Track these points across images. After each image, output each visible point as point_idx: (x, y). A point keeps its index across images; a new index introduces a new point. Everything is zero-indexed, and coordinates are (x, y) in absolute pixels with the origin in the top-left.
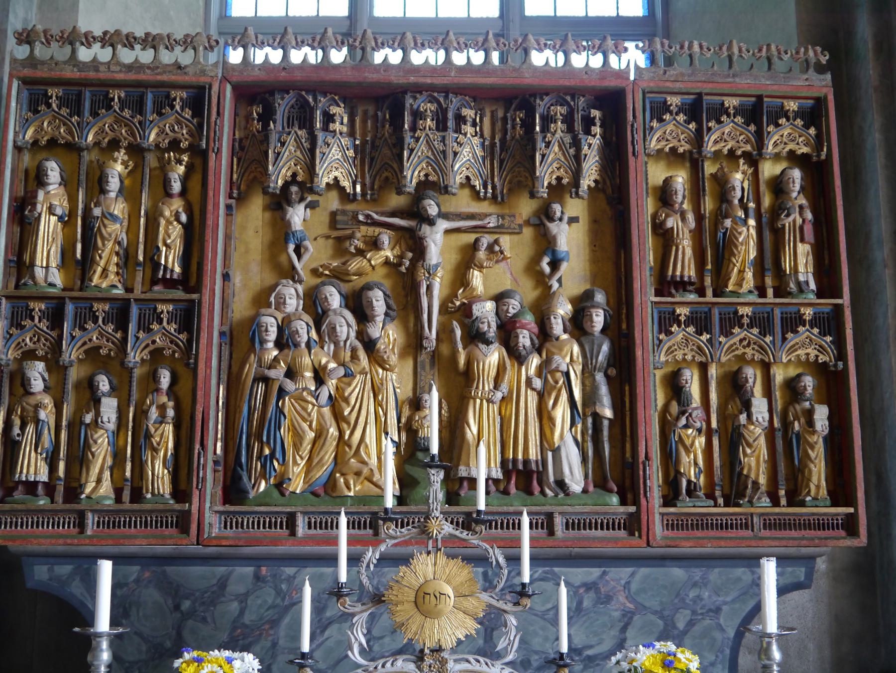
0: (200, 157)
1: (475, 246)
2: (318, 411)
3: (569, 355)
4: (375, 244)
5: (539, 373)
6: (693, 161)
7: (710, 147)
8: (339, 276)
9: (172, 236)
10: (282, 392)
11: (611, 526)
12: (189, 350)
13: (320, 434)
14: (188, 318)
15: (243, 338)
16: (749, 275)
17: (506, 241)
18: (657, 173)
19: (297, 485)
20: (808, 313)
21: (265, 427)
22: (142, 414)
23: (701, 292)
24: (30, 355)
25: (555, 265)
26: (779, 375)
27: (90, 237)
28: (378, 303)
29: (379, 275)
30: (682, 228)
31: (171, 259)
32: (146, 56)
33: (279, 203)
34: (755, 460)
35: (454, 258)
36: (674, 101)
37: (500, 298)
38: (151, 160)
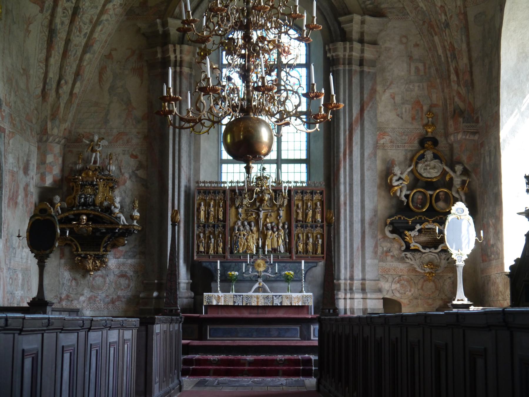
0: (225, 202)
1: (267, 215)
2: (244, 240)
3: (282, 233)
4: (252, 215)
5: (277, 234)
6: (302, 200)
7: (305, 198)
8: (247, 219)
9: (221, 213)
10: (238, 238)
11: (287, 257)
12: (224, 231)
13: (244, 244)
14: (224, 227)
15: (232, 229)
16: (310, 219)
17: (272, 214)
18: (296, 202)
19: (241, 252)
20: (319, 225)
21: (236, 243)
22: (217, 241)
23: (303, 222)
24: (201, 232)
25: (280, 218)
26: (315, 235)
27: (209, 213)
28: (253, 224)
29: (253, 220)
30: (300, 212)
31: (221, 217)
32: (216, 185)
33: (237, 208)
34: (310, 248)
35: (264, 216)
36: (299, 191)
37: (271, 223)
38: (217, 201)
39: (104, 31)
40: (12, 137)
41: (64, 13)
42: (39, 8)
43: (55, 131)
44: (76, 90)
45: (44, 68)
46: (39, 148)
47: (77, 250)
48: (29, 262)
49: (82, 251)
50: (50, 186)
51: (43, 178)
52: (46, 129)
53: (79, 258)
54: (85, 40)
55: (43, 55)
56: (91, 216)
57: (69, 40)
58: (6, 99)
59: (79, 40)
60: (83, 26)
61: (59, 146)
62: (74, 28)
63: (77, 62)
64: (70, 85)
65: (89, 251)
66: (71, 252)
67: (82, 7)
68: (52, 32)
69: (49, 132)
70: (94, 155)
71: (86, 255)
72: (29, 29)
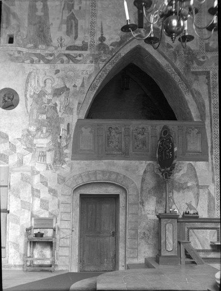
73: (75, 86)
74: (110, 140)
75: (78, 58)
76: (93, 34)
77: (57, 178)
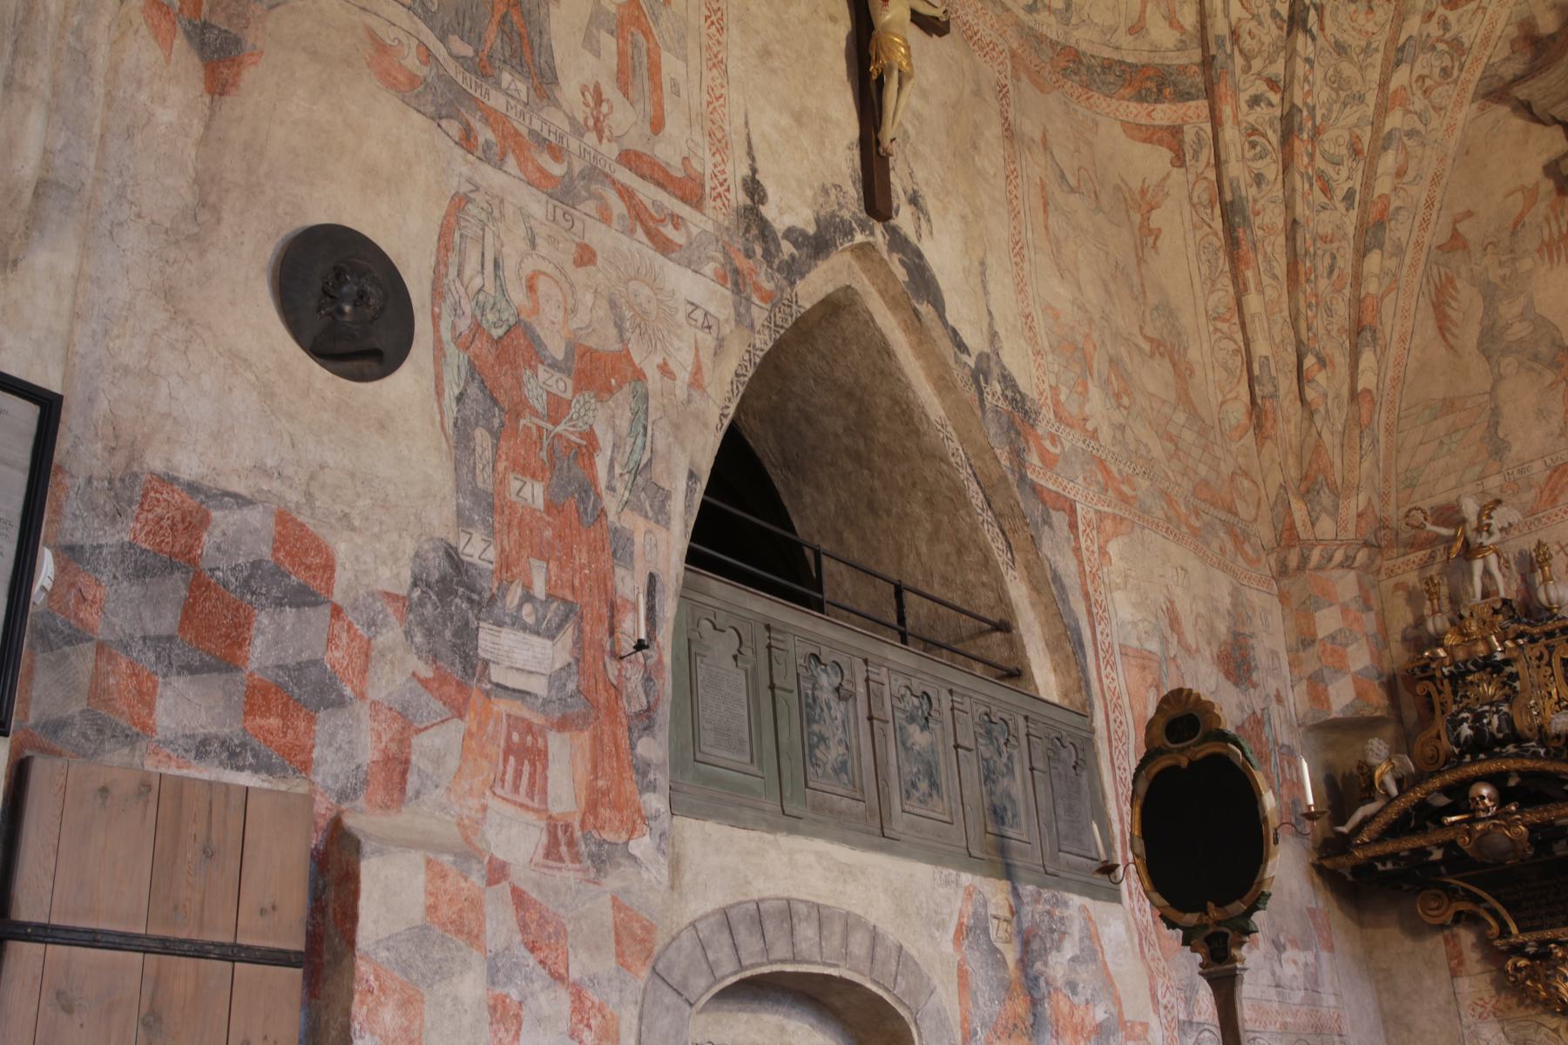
39: (1411, 174)
40: (1116, 534)
41: (1253, 145)
42: (1167, 154)
43: (1326, 527)
44: (1366, 381)
45: (1239, 337)
46: (1283, 598)
47: (1504, 932)
48: (1329, 1000)
49: (1521, 931)
50: (1349, 714)
51: (1317, 692)
52: (1292, 527)
53: (1522, 963)
54: (1354, 213)
55: (1223, 295)
56: (1512, 783)
57: (1295, 221)
58: (1057, 403)
59: (1333, 221)
60: (1330, 170)
61: (1352, 574)
62: (1298, 177)
63: (1347, 291)
64: (1343, 371)
65: (1551, 927)
66: (1484, 943)
67: (1305, 103)
68: (1232, 214)
69: (1302, 536)
70: (1478, 566)
71: (1543, 943)
72: (1153, 225)
73: (664, 369)
74: (815, 727)
75: (668, 231)
76: (720, 146)
77: (609, 922)
